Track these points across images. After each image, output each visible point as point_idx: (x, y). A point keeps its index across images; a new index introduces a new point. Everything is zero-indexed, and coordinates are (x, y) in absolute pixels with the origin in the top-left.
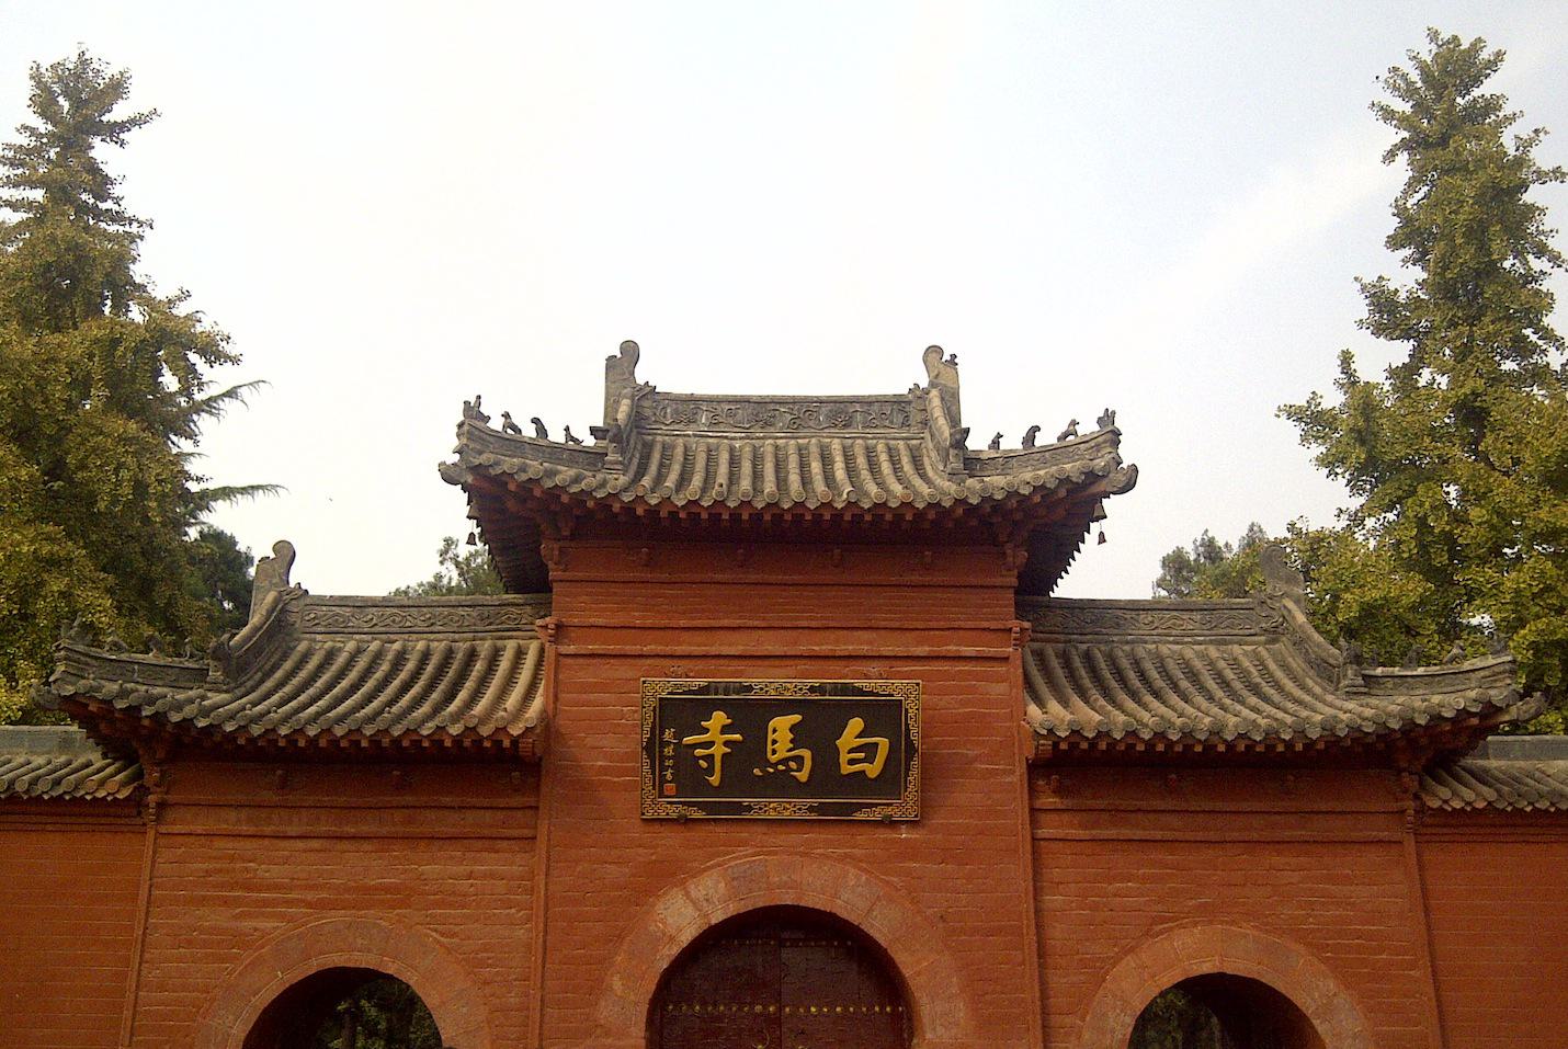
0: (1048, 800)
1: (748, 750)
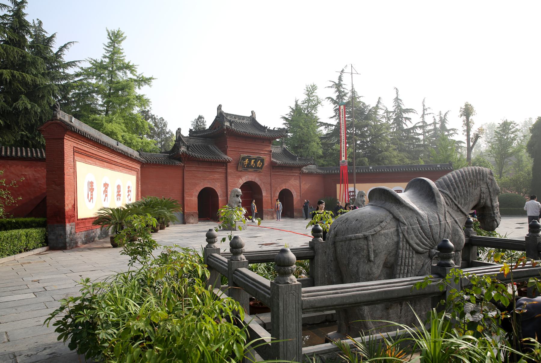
1: (249, 164)
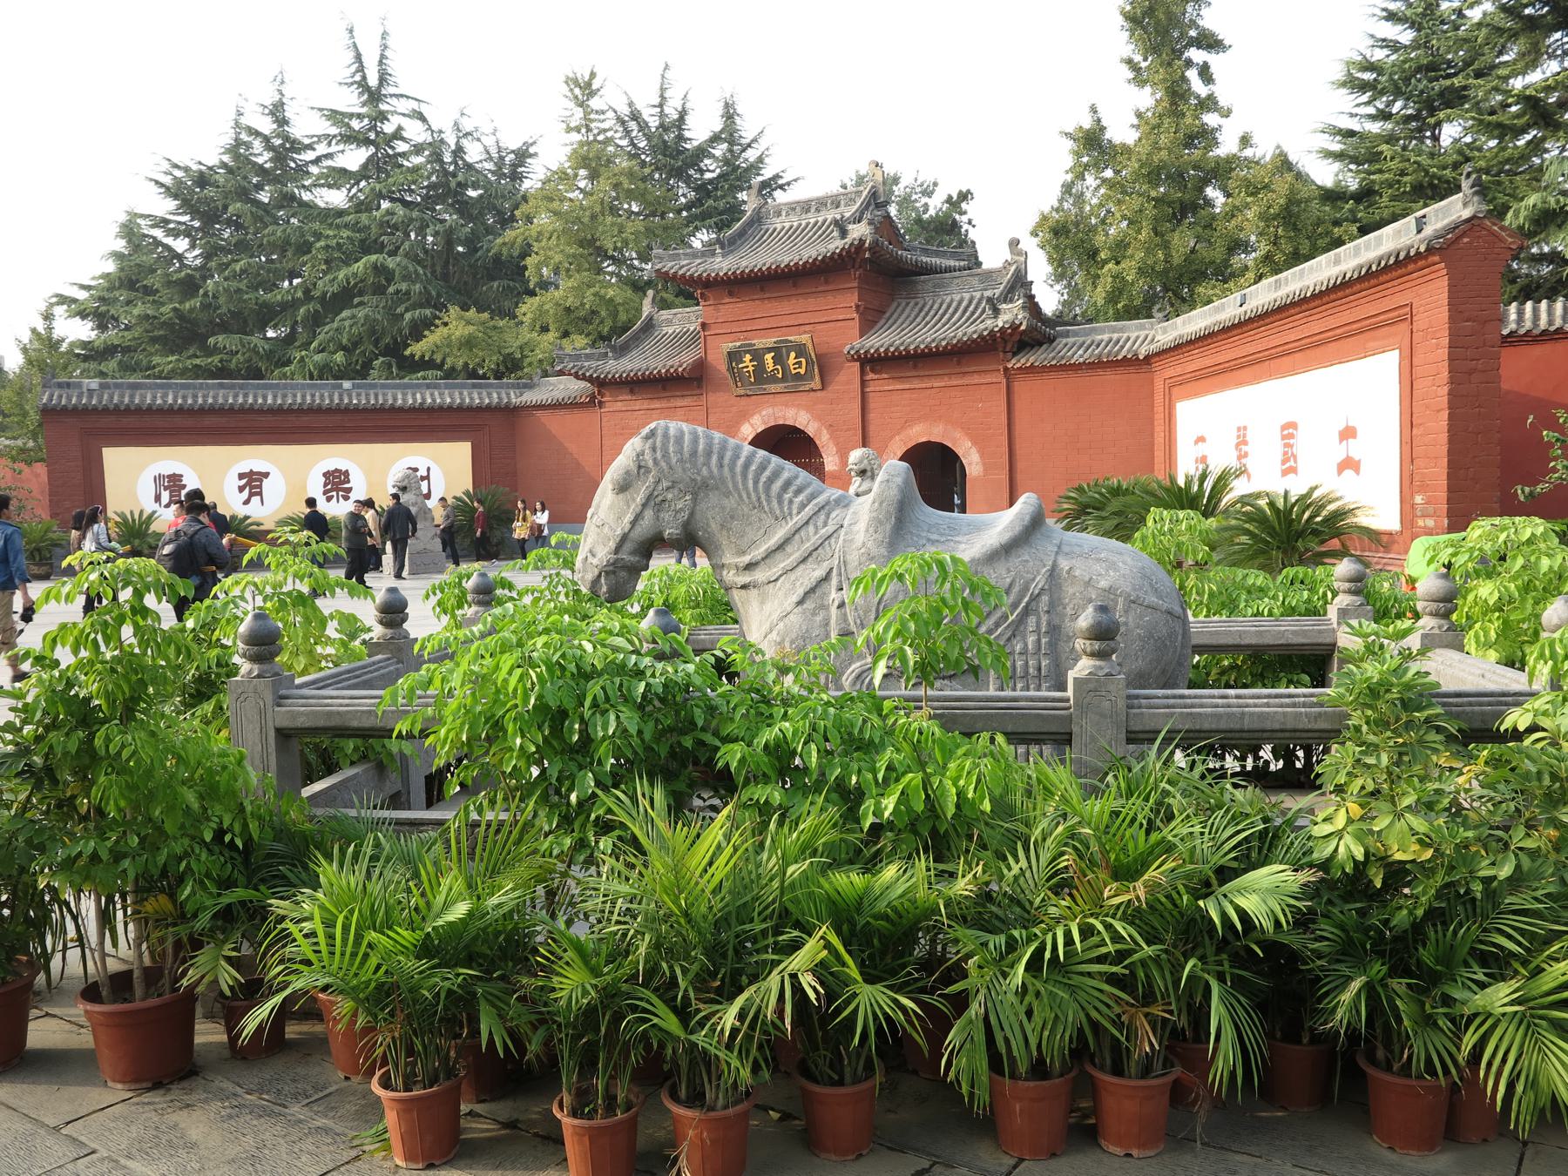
0: (871, 376)
1: (760, 368)
